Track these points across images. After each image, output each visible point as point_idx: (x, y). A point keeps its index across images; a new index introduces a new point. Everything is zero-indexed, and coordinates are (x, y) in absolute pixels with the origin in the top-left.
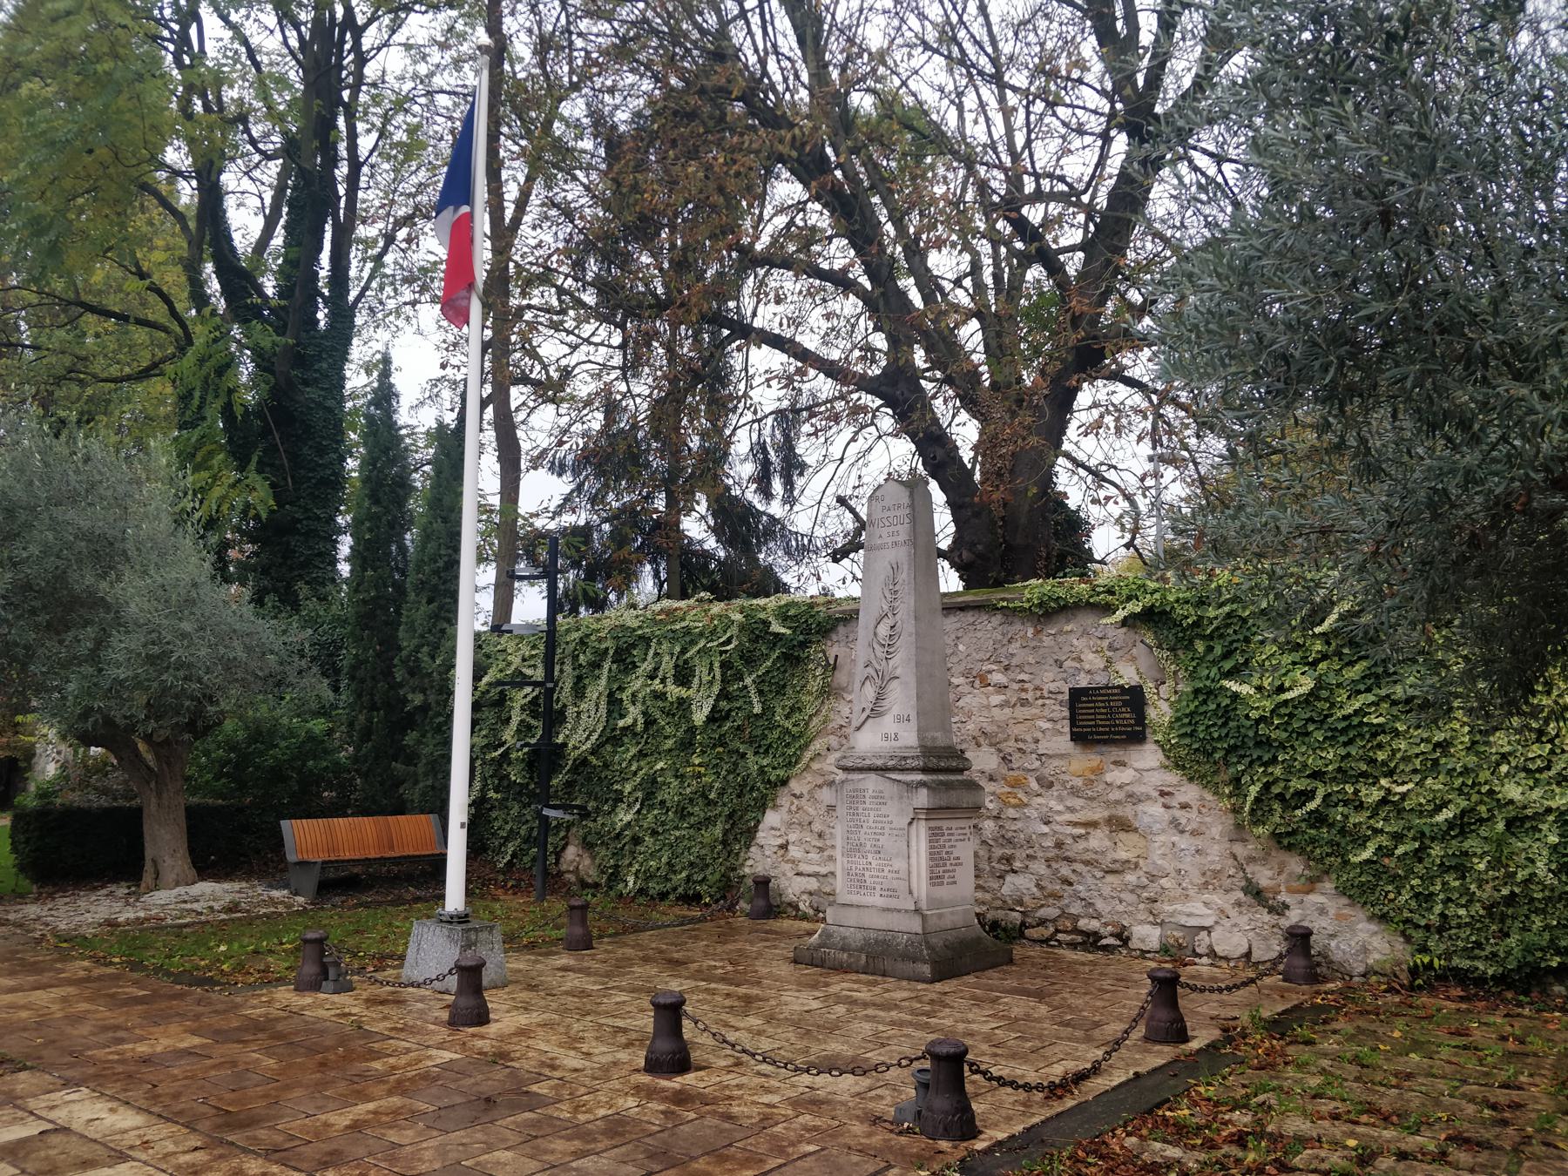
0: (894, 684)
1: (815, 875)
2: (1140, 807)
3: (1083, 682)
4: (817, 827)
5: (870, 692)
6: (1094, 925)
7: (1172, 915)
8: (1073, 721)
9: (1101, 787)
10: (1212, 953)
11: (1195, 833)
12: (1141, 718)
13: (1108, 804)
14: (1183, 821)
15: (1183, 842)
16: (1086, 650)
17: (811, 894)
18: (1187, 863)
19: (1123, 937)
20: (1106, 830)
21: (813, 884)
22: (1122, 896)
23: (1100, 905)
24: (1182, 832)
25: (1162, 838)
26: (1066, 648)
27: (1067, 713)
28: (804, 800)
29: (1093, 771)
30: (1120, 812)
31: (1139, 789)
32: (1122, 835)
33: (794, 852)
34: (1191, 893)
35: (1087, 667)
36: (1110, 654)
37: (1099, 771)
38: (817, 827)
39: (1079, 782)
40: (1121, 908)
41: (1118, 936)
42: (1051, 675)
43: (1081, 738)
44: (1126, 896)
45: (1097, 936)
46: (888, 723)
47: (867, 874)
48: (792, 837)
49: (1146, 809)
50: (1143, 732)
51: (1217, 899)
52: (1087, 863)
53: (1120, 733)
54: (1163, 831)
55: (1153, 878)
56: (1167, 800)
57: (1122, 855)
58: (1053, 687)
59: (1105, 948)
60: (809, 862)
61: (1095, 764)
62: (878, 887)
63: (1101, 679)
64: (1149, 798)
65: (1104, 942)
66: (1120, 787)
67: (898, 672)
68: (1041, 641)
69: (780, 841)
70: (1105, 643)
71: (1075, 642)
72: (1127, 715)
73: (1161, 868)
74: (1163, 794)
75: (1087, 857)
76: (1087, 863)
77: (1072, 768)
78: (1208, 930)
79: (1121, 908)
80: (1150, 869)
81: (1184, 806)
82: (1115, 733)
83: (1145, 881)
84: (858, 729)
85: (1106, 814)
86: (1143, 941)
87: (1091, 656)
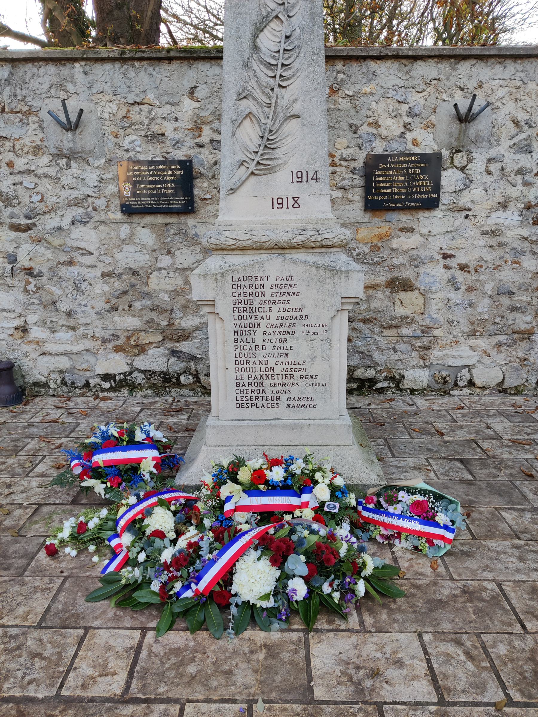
0: (293, 125)
1: (66, 354)
2: (422, 270)
3: (379, 148)
4: (64, 306)
5: (250, 134)
6: (371, 373)
7: (441, 358)
8: (368, 188)
9: (385, 253)
10: (471, 384)
11: (470, 289)
12: (437, 188)
13: (391, 268)
14: (460, 279)
15: (454, 296)
16: (385, 115)
17: (61, 372)
18: (459, 315)
19: (397, 381)
20: (387, 291)
21: (64, 363)
22: (398, 347)
23: (377, 356)
24: (457, 289)
25: (439, 295)
26: (363, 113)
27: (359, 181)
28: (44, 279)
29: (380, 237)
30: (402, 274)
31: (423, 253)
32: (403, 295)
33: (35, 333)
34: (460, 339)
35: (384, 133)
36: (409, 120)
37: (385, 237)
38: (64, 306)
39: (366, 249)
40: (395, 357)
41: (392, 379)
42: (344, 142)
43: (374, 206)
44: (401, 346)
45: (372, 381)
46: (281, 183)
47: (267, 382)
48: (32, 318)
49: (428, 271)
50: (438, 200)
51: (483, 343)
52: (366, 321)
53: (416, 201)
54: (441, 289)
55: (426, 330)
56: (448, 262)
57: (401, 311)
58: (346, 153)
59: (381, 391)
60: (58, 342)
61: (383, 231)
63: (396, 147)
64: (432, 259)
65: (379, 385)
66: (404, 252)
67: (297, 109)
68: (336, 103)
69: (17, 323)
70: (405, 108)
73: (435, 321)
74: (445, 256)
75: (367, 316)
76: (366, 321)
77: (359, 236)
78: (469, 368)
79: (395, 357)
80: (427, 322)
81: (463, 268)
82: (411, 201)
83: (418, 332)
84: (233, 191)
85: (389, 277)
86: (414, 381)
87: (389, 122)
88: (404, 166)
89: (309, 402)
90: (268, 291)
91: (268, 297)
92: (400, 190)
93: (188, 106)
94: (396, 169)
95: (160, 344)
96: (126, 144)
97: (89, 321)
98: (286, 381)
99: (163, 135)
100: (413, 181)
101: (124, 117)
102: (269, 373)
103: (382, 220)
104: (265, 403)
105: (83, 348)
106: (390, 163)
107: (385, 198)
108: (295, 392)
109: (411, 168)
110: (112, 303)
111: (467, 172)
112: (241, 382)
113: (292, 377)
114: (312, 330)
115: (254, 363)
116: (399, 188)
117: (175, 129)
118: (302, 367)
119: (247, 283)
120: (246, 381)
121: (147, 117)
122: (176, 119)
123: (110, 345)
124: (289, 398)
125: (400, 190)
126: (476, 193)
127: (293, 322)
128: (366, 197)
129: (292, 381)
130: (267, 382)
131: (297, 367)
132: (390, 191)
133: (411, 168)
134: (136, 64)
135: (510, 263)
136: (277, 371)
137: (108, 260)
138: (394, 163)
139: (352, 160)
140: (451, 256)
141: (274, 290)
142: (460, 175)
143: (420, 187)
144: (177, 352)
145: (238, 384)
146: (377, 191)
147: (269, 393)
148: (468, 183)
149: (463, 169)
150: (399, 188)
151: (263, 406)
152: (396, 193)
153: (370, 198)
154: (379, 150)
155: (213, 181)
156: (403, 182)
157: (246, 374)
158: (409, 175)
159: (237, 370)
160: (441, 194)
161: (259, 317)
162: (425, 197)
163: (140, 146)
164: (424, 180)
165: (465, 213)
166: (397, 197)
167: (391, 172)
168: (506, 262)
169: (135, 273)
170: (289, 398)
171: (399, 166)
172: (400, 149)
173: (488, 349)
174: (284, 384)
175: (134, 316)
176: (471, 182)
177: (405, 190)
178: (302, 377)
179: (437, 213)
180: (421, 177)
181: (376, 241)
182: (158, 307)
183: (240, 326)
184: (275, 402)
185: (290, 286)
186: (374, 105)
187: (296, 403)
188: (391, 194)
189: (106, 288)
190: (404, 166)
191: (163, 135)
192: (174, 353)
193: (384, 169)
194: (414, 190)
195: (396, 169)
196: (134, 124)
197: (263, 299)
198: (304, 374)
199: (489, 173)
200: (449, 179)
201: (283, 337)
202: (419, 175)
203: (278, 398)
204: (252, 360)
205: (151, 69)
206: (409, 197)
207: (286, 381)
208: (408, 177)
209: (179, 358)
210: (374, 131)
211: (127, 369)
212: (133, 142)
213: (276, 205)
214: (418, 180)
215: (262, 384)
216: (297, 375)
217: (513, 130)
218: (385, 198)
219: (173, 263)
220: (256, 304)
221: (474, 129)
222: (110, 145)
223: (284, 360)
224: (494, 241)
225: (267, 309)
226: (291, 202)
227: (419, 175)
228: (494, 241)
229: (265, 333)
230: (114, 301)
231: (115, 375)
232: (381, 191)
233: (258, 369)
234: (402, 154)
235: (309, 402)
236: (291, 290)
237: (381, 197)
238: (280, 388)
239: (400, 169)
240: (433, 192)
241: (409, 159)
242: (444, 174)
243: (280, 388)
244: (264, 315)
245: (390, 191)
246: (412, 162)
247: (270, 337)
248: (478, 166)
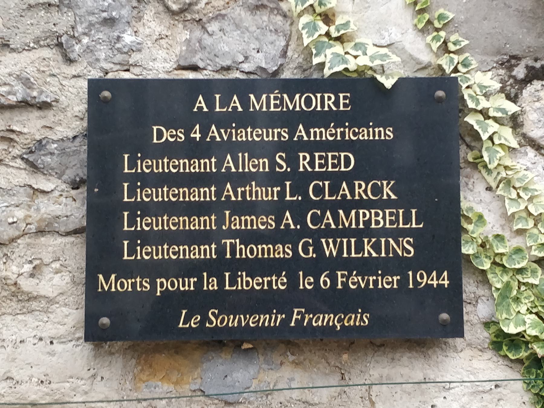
8: (102, 241)
53: (339, 301)
72: (384, 220)
88: (272, 135)
92: (261, 250)
94: (233, 148)
100: (323, 205)
103: (186, 389)
106: (207, 120)
107: (188, 285)
109: (312, 147)
116: (250, 237)
125: (261, 250)
128: (91, 283)
132: (209, 251)
133: (312, 147)
138: (224, 122)
139: (25, 105)
143: (360, 234)
146: (144, 254)
152: (237, 266)
153: (111, 284)
154: (158, 63)
158: (301, 181)
162: (389, 282)
164: (389, 203)
166: (247, 282)
167: (209, 165)
171: (243, 135)
172: (259, 60)
177: (282, 252)
180: (362, 189)
188: (217, 267)
190: (272, 135)
193: (170, 150)
194: (330, 249)
195: (233, 148)
202: (349, 177)
206: (306, 283)
208: (299, 188)
214: (348, 205)
218: (188, 285)
227: (349, 177)
232: (167, 252)
237: (163, 284)
239: (254, 149)
240: (425, 261)
241: (298, 102)
245: (209, 251)
246: (313, 119)
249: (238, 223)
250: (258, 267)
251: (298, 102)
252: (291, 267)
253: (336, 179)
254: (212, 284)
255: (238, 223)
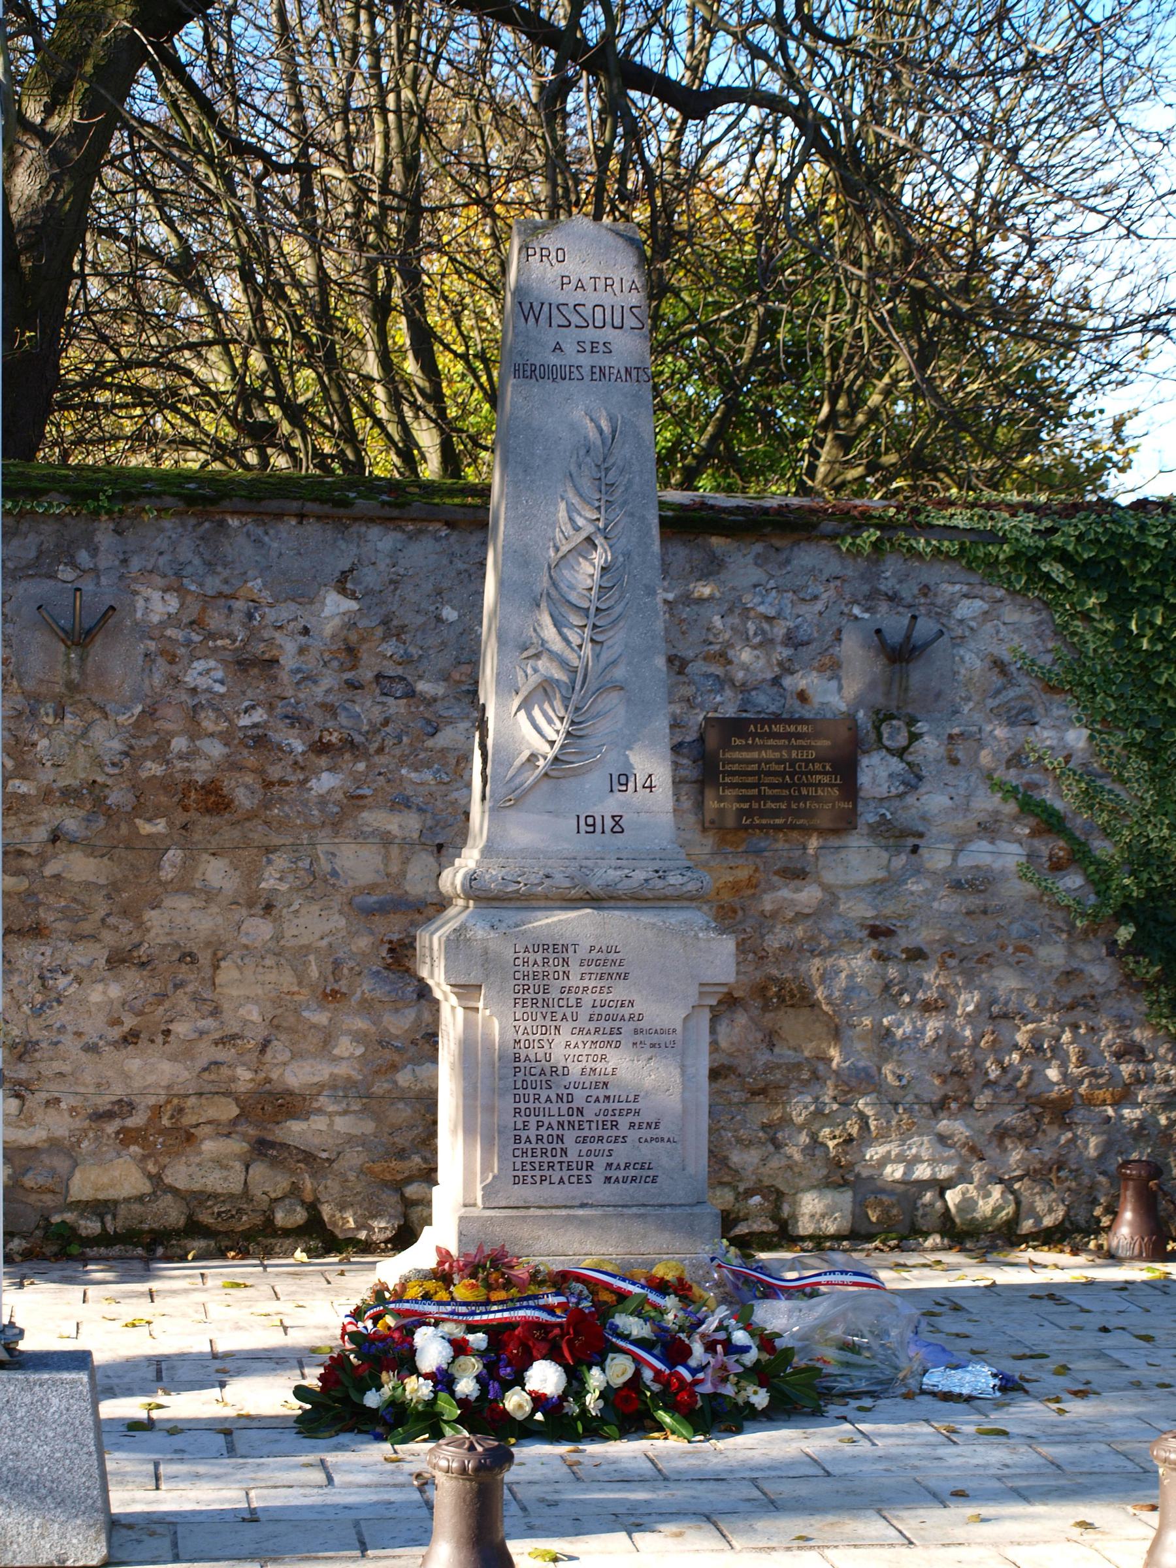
29: (735, 887)
47: (570, 1136)
61: (743, 874)
62: (600, 1163)
63: (764, 701)
70: (779, 631)
71: (717, 621)
74: (876, 932)
87: (746, 656)
89: (645, 1173)
90: (575, 970)
91: (574, 981)
93: (335, 607)
95: (226, 1130)
96: (191, 678)
97: (66, 1068)
98: (605, 1134)
99: (274, 661)
101: (192, 623)
102: (574, 1118)
104: (565, 1174)
105: (43, 1134)
106: (755, 735)
108: (622, 1153)
110: (126, 1028)
111: (910, 758)
112: (524, 1135)
113: (615, 1125)
114: (649, 1039)
115: (549, 1100)
117: (302, 651)
118: (632, 1106)
119: (539, 957)
120: (532, 1133)
121: (244, 625)
122: (306, 631)
123: (111, 1128)
124: (610, 1165)
125: (776, 791)
126: (933, 801)
127: (617, 1024)
129: (614, 1133)
130: (570, 1136)
131: (625, 1106)
134: (234, 522)
135: (1010, 950)
136: (589, 1114)
137: (126, 926)
138: (761, 736)
140: (889, 933)
141: (584, 969)
142: (896, 765)
144: (273, 1145)
145: (517, 1139)
147: (572, 1156)
148: (914, 781)
149: (901, 753)
150: (772, 786)
151: (561, 1181)
152: (766, 798)
154: (730, 711)
155: (376, 759)
156: (782, 774)
157: (533, 1120)
158: (793, 763)
159: (517, 1112)
160: (860, 804)
161: (559, 1016)
163: (222, 682)
164: (825, 773)
165: (911, 841)
166: (771, 805)
168: (1003, 948)
169: (188, 958)
170: (610, 1165)
171: (771, 742)
173: (981, 1142)
174: (600, 1139)
175: (173, 1058)
176: (920, 778)
177: (786, 792)
178: (632, 1125)
179: (856, 841)
180: (818, 767)
181: (726, 897)
182: (234, 1037)
183: (525, 1031)
184: (584, 1172)
185: (614, 962)
186: (717, 621)
187: (621, 1174)
189: (115, 991)
191: (274, 661)
192: (262, 1148)
196: (212, 636)
197: (566, 983)
198: (637, 1120)
199: (954, 761)
200: (876, 773)
201: (599, 1051)
202: (813, 761)
203: (590, 1166)
204: (544, 1095)
205: (260, 531)
207: (605, 1134)
209: (274, 1163)
210: (718, 670)
211: (146, 1187)
212: (208, 671)
213: (583, 827)
215: (560, 1138)
216: (624, 1122)
217: (997, 680)
219: (278, 937)
220: (554, 994)
221: (917, 675)
222: (157, 680)
223: (601, 1093)
224: (974, 901)
225: (572, 1002)
226: (609, 823)
228: (974, 901)
229: (568, 1045)
230: (129, 1022)
231: (116, 1203)
233: (554, 1111)
234: (777, 719)
235: (645, 1173)
236: (614, 970)
238: (593, 1146)
241: (792, 729)
242: (865, 761)
243: (593, 1146)
244: (568, 1012)
245: (755, 792)
247: (577, 1052)
248: (930, 746)
249: (767, 780)
250: (775, 799)
251: (792, 729)
252: (790, 798)
253: (807, 761)
254: (755, 806)
255: (767, 780)
